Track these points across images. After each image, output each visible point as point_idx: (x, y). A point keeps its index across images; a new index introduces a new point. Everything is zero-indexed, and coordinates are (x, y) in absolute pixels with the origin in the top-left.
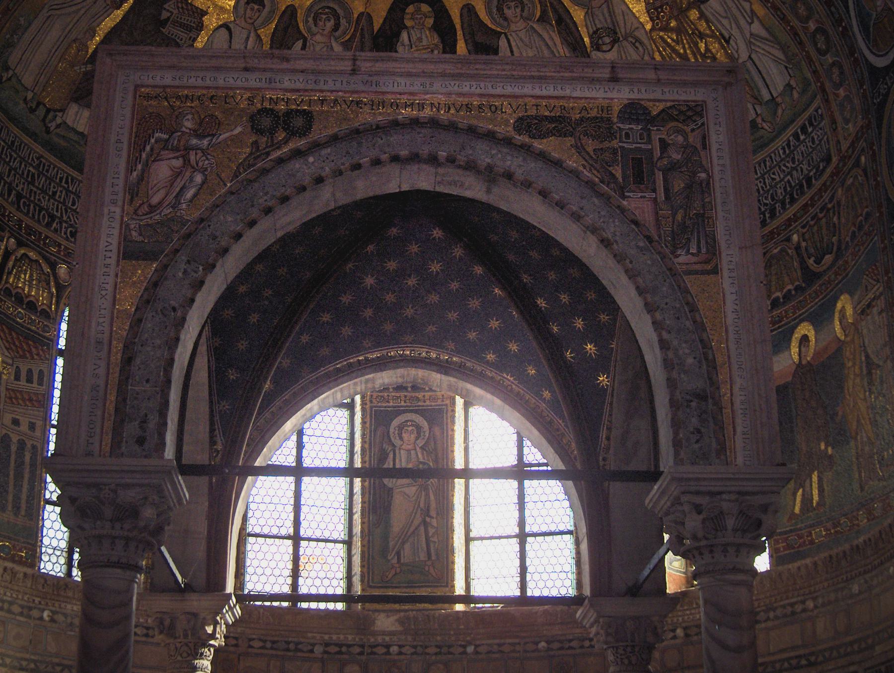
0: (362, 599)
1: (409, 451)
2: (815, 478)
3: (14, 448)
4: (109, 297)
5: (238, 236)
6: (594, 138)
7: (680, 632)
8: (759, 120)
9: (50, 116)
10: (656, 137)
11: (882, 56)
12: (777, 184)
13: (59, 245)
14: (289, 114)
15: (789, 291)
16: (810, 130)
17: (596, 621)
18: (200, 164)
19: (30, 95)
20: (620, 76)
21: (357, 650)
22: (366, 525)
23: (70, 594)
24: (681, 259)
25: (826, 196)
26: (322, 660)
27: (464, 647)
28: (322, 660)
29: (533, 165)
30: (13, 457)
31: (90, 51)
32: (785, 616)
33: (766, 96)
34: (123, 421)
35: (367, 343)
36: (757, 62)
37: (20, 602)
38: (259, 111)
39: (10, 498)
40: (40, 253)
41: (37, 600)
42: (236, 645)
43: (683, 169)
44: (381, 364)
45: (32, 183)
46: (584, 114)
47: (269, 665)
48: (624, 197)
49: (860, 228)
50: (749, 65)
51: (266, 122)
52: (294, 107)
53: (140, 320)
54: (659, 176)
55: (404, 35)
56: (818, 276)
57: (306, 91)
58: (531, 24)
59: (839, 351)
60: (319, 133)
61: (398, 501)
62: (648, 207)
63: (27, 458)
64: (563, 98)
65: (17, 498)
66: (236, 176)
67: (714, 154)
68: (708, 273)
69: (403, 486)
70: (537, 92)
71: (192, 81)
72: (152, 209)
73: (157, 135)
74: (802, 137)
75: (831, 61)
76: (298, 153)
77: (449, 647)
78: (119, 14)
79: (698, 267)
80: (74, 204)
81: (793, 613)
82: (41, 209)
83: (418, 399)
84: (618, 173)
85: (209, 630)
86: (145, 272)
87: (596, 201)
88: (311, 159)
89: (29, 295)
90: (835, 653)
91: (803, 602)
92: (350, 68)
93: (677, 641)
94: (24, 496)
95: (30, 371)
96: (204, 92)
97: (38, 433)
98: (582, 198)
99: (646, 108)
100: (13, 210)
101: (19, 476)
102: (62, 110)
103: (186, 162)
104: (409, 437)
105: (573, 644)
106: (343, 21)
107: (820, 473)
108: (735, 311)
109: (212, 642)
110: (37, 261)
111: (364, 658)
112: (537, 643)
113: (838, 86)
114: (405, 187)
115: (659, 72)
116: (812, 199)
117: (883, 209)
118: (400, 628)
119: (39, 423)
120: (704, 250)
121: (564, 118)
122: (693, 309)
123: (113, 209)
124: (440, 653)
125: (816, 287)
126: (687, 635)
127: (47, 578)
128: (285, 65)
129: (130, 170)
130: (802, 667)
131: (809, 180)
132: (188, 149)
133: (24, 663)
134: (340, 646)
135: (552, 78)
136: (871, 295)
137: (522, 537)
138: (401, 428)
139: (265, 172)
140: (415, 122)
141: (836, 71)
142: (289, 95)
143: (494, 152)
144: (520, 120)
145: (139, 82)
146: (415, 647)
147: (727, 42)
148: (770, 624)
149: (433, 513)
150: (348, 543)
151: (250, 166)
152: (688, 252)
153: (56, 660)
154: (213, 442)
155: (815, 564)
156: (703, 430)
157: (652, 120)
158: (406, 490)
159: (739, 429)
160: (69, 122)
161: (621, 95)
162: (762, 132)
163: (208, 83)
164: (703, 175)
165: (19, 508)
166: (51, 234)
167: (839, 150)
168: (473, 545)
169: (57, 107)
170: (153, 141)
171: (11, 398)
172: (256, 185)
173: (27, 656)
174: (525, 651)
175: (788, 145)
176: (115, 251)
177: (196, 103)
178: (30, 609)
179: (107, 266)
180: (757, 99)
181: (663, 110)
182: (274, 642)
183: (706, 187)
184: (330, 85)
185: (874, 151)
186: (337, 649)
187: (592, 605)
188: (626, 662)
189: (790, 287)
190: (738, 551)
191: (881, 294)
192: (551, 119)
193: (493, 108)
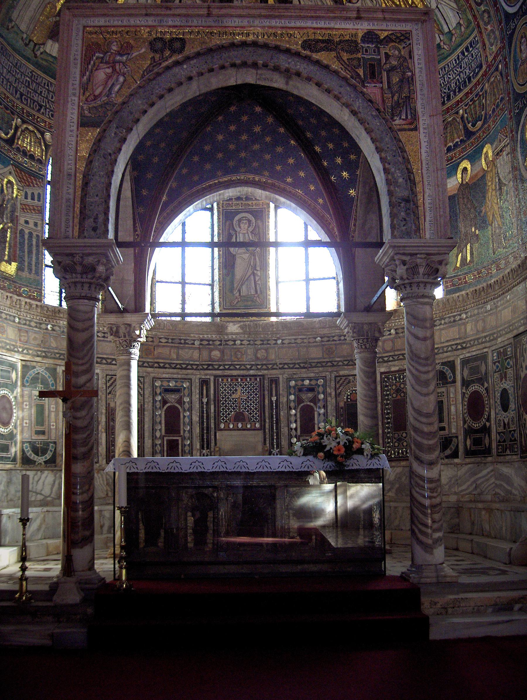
0: (220, 315)
1: (244, 234)
2: (468, 247)
3: (26, 237)
4: (74, 149)
5: (145, 112)
6: (347, 52)
7: (393, 331)
8: (442, 44)
9: (37, 47)
10: (383, 52)
11: (511, 6)
12: (451, 81)
13: (45, 122)
14: (172, 40)
15: (457, 142)
16: (471, 49)
17: (348, 326)
18: (122, 71)
20: (362, 16)
21: (219, 343)
22: (221, 276)
23: (62, 316)
24: (397, 122)
25: (479, 88)
26: (199, 348)
27: (276, 340)
28: (199, 348)
29: (312, 68)
30: (26, 242)
31: (58, 9)
32: (450, 322)
33: (446, 30)
34: (84, 218)
35: (219, 173)
36: (441, 10)
37: (35, 320)
38: (155, 39)
39: (26, 264)
40: (35, 127)
41: (44, 319)
42: (152, 341)
43: (399, 70)
44: (228, 185)
45: (28, 86)
46: (342, 38)
47: (170, 352)
48: (364, 86)
49: (497, 106)
50: (437, 11)
51: (159, 45)
52: (174, 36)
53: (91, 162)
54: (385, 74)
56: (473, 133)
57: (181, 26)
59: (483, 177)
60: (189, 51)
61: (238, 261)
62: (377, 92)
63: (34, 243)
64: (329, 29)
65: (30, 264)
66: (143, 76)
67: (416, 62)
68: (412, 130)
69: (241, 254)
70: (315, 25)
71: (116, 23)
72: (96, 97)
73: (97, 55)
74: (466, 54)
75: (483, 9)
76: (177, 63)
77: (268, 340)
79: (406, 127)
80: (52, 98)
82: (34, 101)
83: (249, 205)
84: (361, 72)
85: (137, 332)
86: (92, 134)
87: (348, 89)
88: (185, 66)
89: (30, 151)
90: (476, 342)
91: (460, 315)
92: (206, 13)
93: (392, 336)
94: (33, 263)
96: (123, 29)
97: (39, 228)
98: (341, 87)
99: (377, 35)
100: (18, 102)
101: (30, 252)
102: (44, 44)
103: (114, 70)
104: (244, 226)
105: (335, 338)
108: (427, 152)
109: (139, 339)
110: (33, 131)
111: (222, 347)
112: (315, 338)
113: (486, 24)
114: (239, 82)
115: (385, 14)
116: (471, 89)
117: (511, 96)
118: (241, 331)
119: (39, 223)
120: (409, 117)
121: (330, 40)
122: (403, 151)
123: (73, 98)
124: (263, 344)
125: (472, 140)
126: (397, 333)
128: (168, 12)
130: (458, 349)
131: (469, 79)
132: (115, 62)
133: (39, 353)
134: (208, 341)
135: (323, 17)
136: (502, 144)
137: (308, 280)
138: (240, 221)
139: (159, 74)
140: (244, 44)
141: (486, 15)
142: (171, 29)
143: (290, 61)
144: (305, 42)
145: (85, 24)
146: (249, 341)
148: (442, 327)
149: (258, 268)
150: (212, 285)
151: (151, 71)
152: (400, 118)
153: (56, 351)
154: (135, 231)
155: (467, 294)
156: (407, 219)
157: (381, 42)
158: (243, 256)
159: (428, 219)
160: (48, 51)
161: (364, 26)
162: (442, 51)
163: (125, 23)
164: (410, 74)
165: (31, 270)
166: (40, 116)
167: (487, 62)
169: (40, 42)
170: (95, 58)
171: (23, 209)
172: (154, 82)
173: (41, 349)
174: (309, 342)
175: (458, 58)
176: (76, 122)
177: (119, 35)
178: (41, 324)
179: (71, 131)
180: (441, 32)
181: (387, 36)
182: (172, 339)
183: (411, 80)
184: (195, 23)
185: (506, 62)
186: (207, 343)
187: (345, 317)
188: (363, 347)
189: (458, 140)
190: (425, 286)
191: (508, 144)
192: (323, 41)
193: (289, 35)
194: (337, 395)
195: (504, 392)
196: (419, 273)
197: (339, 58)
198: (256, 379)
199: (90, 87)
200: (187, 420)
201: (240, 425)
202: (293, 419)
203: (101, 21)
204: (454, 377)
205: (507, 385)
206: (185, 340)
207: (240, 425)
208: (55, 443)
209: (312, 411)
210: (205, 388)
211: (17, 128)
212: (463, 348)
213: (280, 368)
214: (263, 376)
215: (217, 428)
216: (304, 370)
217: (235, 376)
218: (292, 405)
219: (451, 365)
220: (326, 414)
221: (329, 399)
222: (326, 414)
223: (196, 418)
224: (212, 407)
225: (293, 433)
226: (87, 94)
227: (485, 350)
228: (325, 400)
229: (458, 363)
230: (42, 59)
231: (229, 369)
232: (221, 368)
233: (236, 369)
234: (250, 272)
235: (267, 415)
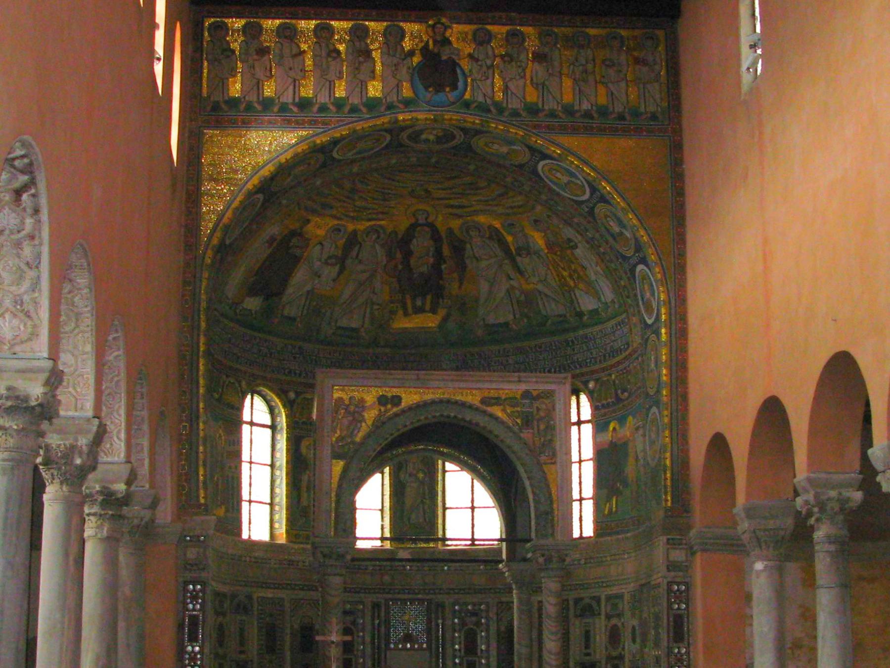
2: (614, 500)
6: (512, 406)
8: (600, 310)
14: (393, 397)
19: (231, 301)
25: (627, 363)
46: (507, 396)
48: (521, 432)
54: (536, 423)
55: (415, 240)
58: (484, 239)
61: (408, 490)
74: (619, 327)
76: (396, 415)
78: (271, 250)
79: (549, 461)
81: (602, 561)
84: (519, 421)
91: (606, 557)
95: (234, 441)
102: (242, 302)
106: (382, 236)
107: (617, 498)
113: (634, 315)
127: (252, 545)
129: (333, 422)
139: (384, 423)
141: (632, 310)
147: (586, 269)
149: (427, 497)
150: (382, 510)
155: (611, 540)
158: (413, 485)
160: (245, 306)
161: (524, 387)
163: (360, 384)
168: (448, 512)
180: (599, 299)
187: (506, 566)
189: (609, 400)
194: (499, 620)
195: (634, 628)
196: (552, 561)
197: (504, 410)
198: (423, 603)
199: (338, 432)
200: (360, 640)
201: (409, 646)
202: (457, 640)
203: (345, 382)
204: (600, 610)
205: (635, 622)
206: (359, 566)
207: (409, 646)
208: (251, 661)
209: (475, 634)
210: (376, 610)
211: (224, 382)
212: (607, 586)
213: (446, 593)
214: (430, 602)
215: (387, 648)
216: (468, 596)
217: (405, 600)
218: (457, 628)
219: (598, 600)
220: (487, 637)
221: (491, 623)
222: (487, 637)
223: (368, 639)
224: (383, 629)
225: (458, 654)
226: (337, 435)
227: (623, 590)
228: (488, 625)
229: (603, 597)
230: (240, 315)
231: (399, 593)
232: (392, 592)
233: (404, 593)
234: (419, 501)
235: (434, 636)
